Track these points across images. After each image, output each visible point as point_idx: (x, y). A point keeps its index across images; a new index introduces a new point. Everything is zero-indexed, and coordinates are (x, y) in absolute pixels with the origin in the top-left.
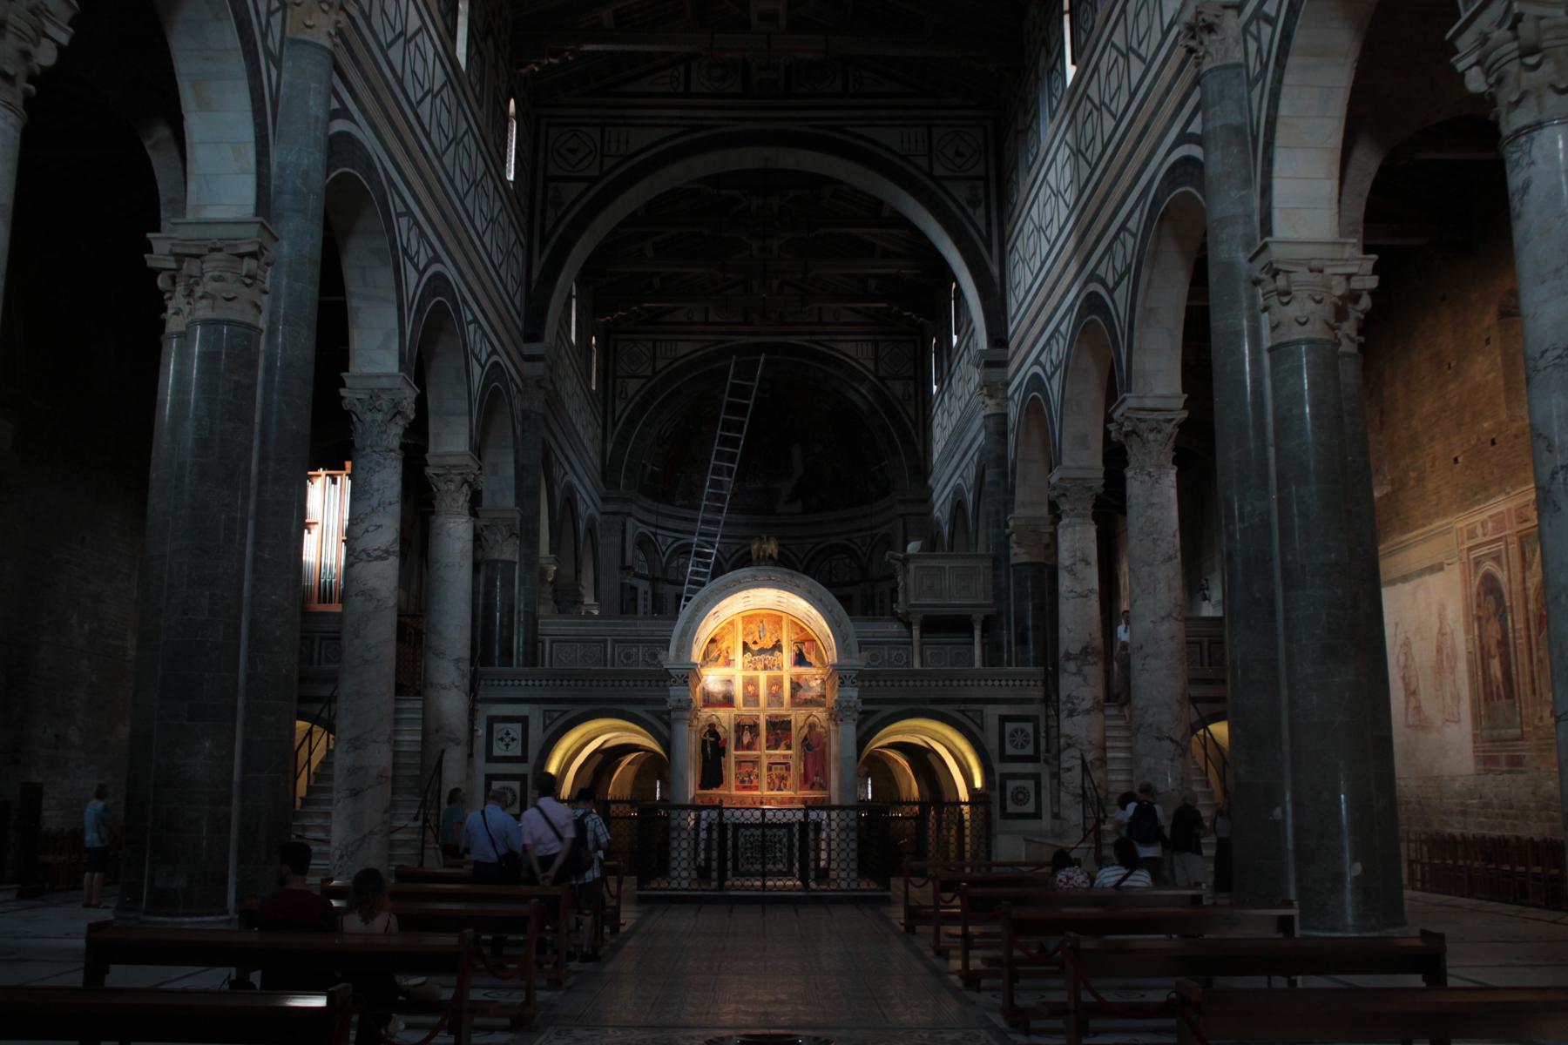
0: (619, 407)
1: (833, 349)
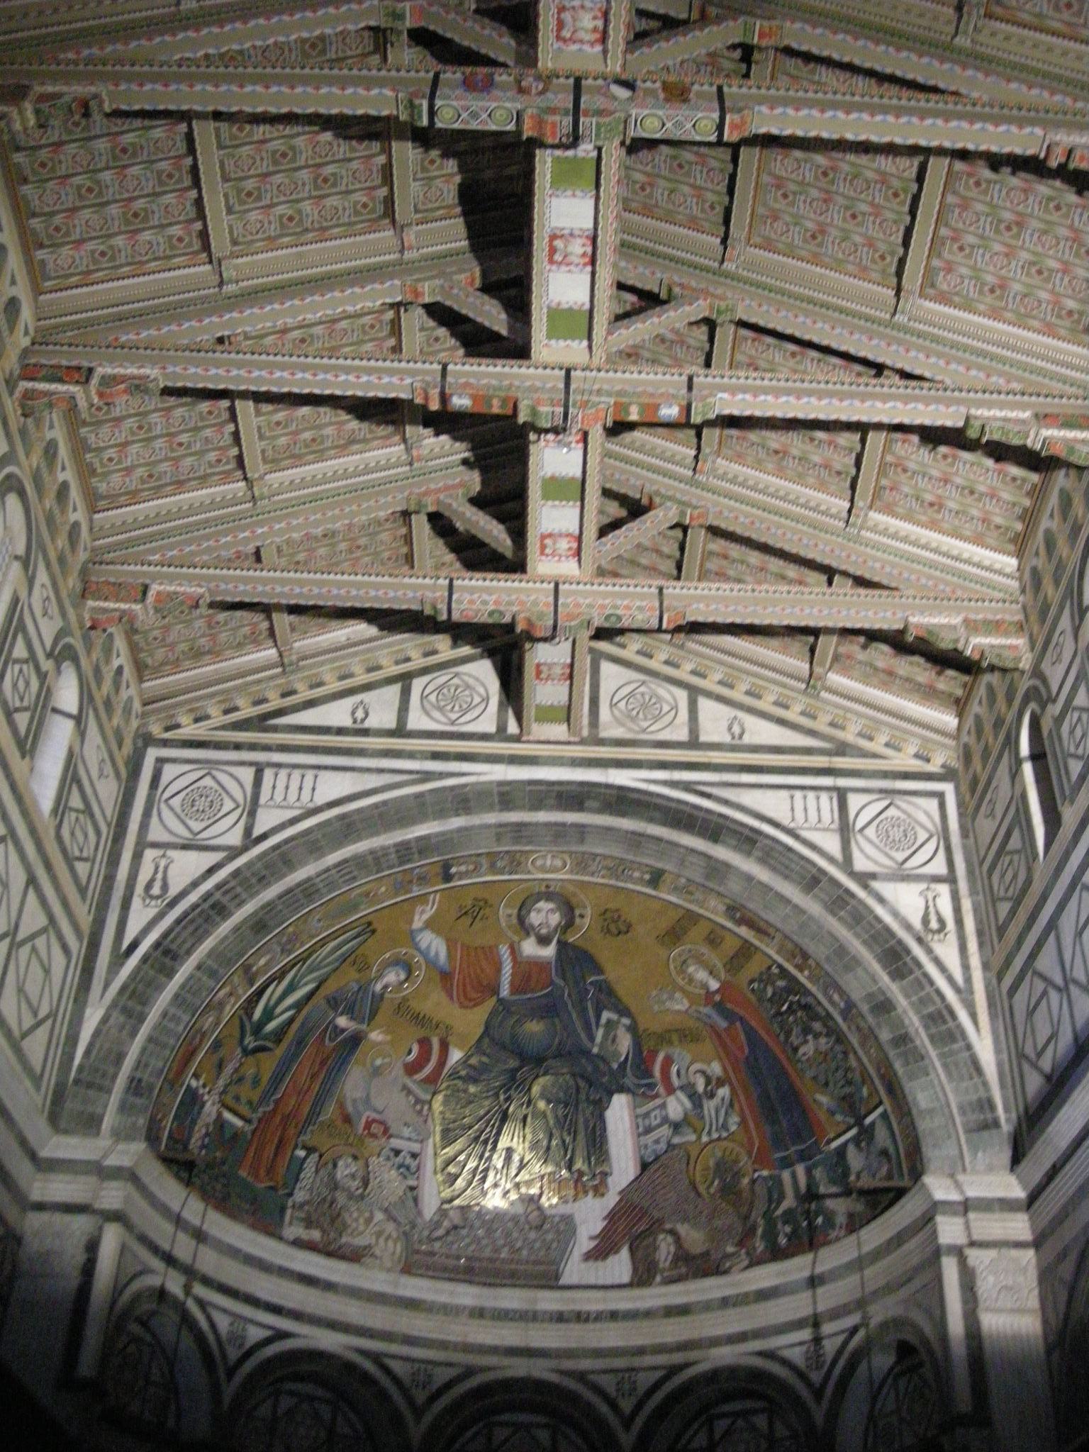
0: (139, 915)
1: (726, 802)
